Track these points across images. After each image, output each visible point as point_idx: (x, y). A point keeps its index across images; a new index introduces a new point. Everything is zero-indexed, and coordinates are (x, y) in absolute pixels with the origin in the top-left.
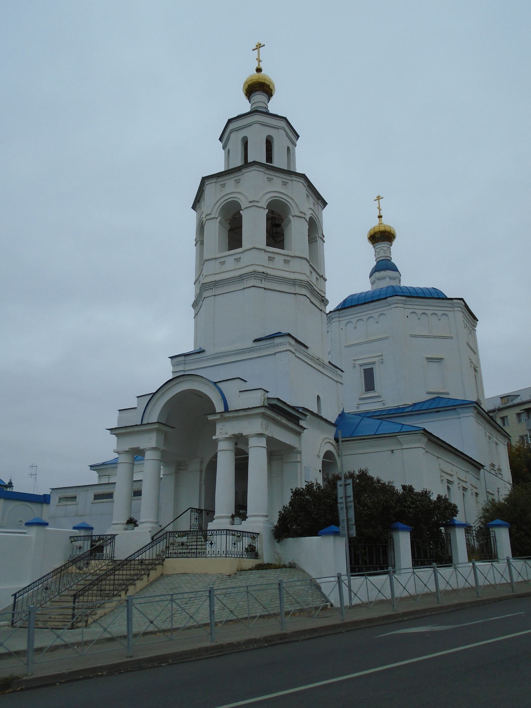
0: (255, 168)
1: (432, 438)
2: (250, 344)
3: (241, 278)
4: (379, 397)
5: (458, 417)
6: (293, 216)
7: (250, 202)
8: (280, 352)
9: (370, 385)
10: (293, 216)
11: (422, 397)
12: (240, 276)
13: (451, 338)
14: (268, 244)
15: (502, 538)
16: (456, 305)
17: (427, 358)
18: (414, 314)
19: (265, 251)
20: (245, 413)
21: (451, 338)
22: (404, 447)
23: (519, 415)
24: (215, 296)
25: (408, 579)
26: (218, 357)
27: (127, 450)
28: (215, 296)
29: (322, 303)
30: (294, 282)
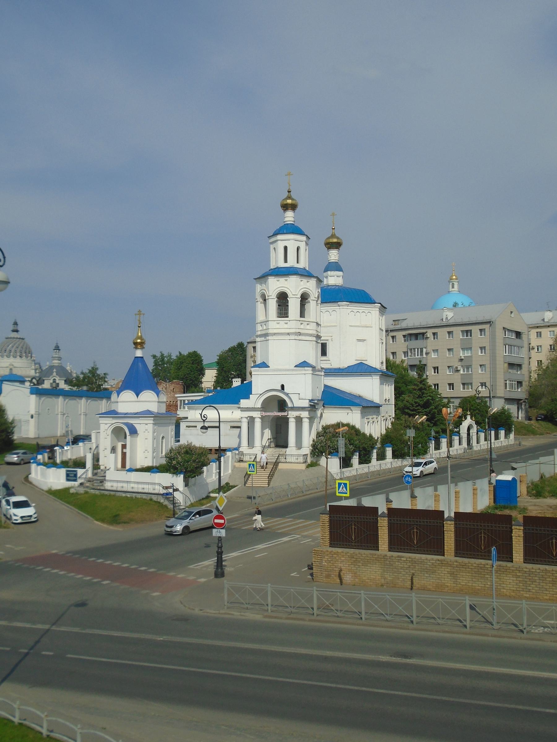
2: (292, 367)
3: (288, 334)
9: (324, 352)
11: (352, 362)
15: (389, 452)
20: (303, 409)
21: (371, 327)
23: (404, 336)
30: (311, 335)
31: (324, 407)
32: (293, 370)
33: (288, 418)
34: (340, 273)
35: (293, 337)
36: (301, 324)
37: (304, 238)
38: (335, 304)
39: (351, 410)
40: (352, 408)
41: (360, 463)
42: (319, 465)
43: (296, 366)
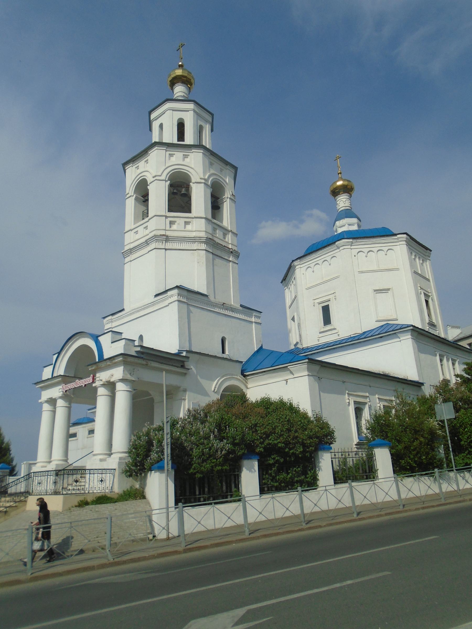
0: (156, 148)
1: (324, 364)
2: (152, 299)
3: (147, 243)
4: (335, 329)
5: (398, 340)
6: (193, 183)
7: (153, 177)
8: (172, 303)
9: (327, 320)
10: (193, 183)
12: (146, 241)
13: (397, 269)
14: (170, 210)
15: (383, 458)
16: (400, 240)
17: (375, 291)
18: (371, 252)
19: (166, 217)
21: (397, 269)
22: (295, 376)
24: (131, 261)
25: (255, 505)
26: (133, 313)
27: (46, 400)
28: (131, 261)
29: (231, 254)
30: (193, 240)
31: (245, 376)
32: (153, 304)
33: (96, 389)
34: (355, 220)
35: (153, 245)
36: (171, 223)
37: (191, 106)
38: (333, 247)
39: (292, 373)
40: (292, 367)
41: (264, 489)
42: (144, 497)
43: (156, 296)
